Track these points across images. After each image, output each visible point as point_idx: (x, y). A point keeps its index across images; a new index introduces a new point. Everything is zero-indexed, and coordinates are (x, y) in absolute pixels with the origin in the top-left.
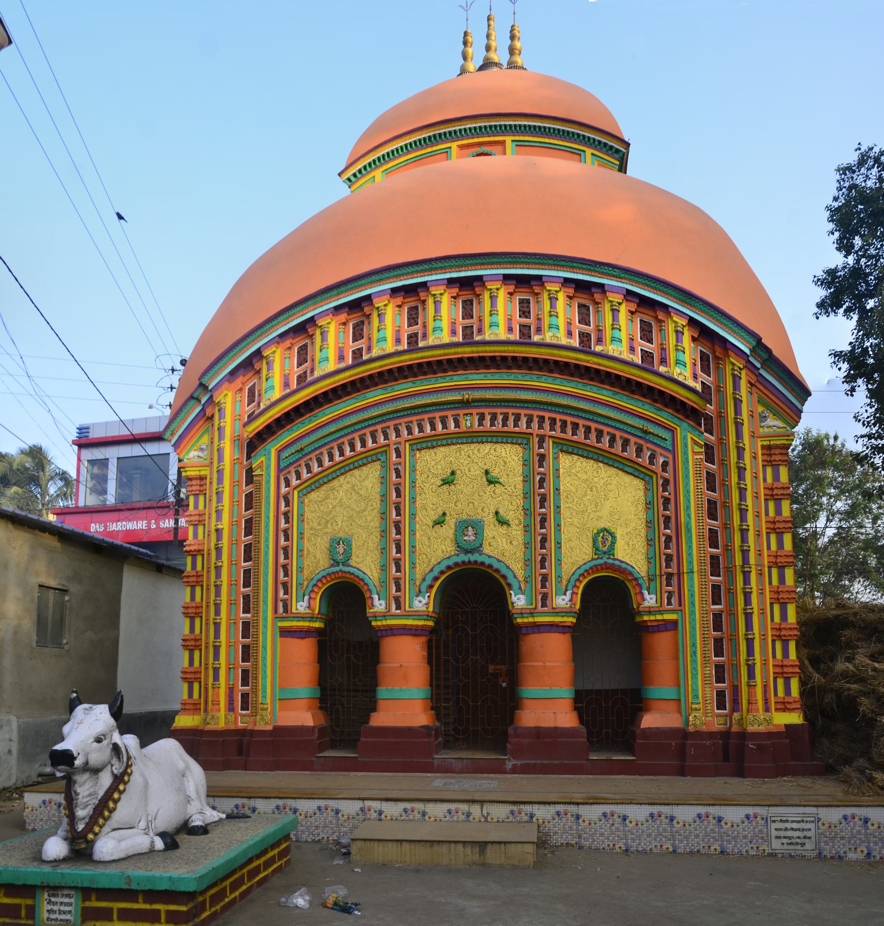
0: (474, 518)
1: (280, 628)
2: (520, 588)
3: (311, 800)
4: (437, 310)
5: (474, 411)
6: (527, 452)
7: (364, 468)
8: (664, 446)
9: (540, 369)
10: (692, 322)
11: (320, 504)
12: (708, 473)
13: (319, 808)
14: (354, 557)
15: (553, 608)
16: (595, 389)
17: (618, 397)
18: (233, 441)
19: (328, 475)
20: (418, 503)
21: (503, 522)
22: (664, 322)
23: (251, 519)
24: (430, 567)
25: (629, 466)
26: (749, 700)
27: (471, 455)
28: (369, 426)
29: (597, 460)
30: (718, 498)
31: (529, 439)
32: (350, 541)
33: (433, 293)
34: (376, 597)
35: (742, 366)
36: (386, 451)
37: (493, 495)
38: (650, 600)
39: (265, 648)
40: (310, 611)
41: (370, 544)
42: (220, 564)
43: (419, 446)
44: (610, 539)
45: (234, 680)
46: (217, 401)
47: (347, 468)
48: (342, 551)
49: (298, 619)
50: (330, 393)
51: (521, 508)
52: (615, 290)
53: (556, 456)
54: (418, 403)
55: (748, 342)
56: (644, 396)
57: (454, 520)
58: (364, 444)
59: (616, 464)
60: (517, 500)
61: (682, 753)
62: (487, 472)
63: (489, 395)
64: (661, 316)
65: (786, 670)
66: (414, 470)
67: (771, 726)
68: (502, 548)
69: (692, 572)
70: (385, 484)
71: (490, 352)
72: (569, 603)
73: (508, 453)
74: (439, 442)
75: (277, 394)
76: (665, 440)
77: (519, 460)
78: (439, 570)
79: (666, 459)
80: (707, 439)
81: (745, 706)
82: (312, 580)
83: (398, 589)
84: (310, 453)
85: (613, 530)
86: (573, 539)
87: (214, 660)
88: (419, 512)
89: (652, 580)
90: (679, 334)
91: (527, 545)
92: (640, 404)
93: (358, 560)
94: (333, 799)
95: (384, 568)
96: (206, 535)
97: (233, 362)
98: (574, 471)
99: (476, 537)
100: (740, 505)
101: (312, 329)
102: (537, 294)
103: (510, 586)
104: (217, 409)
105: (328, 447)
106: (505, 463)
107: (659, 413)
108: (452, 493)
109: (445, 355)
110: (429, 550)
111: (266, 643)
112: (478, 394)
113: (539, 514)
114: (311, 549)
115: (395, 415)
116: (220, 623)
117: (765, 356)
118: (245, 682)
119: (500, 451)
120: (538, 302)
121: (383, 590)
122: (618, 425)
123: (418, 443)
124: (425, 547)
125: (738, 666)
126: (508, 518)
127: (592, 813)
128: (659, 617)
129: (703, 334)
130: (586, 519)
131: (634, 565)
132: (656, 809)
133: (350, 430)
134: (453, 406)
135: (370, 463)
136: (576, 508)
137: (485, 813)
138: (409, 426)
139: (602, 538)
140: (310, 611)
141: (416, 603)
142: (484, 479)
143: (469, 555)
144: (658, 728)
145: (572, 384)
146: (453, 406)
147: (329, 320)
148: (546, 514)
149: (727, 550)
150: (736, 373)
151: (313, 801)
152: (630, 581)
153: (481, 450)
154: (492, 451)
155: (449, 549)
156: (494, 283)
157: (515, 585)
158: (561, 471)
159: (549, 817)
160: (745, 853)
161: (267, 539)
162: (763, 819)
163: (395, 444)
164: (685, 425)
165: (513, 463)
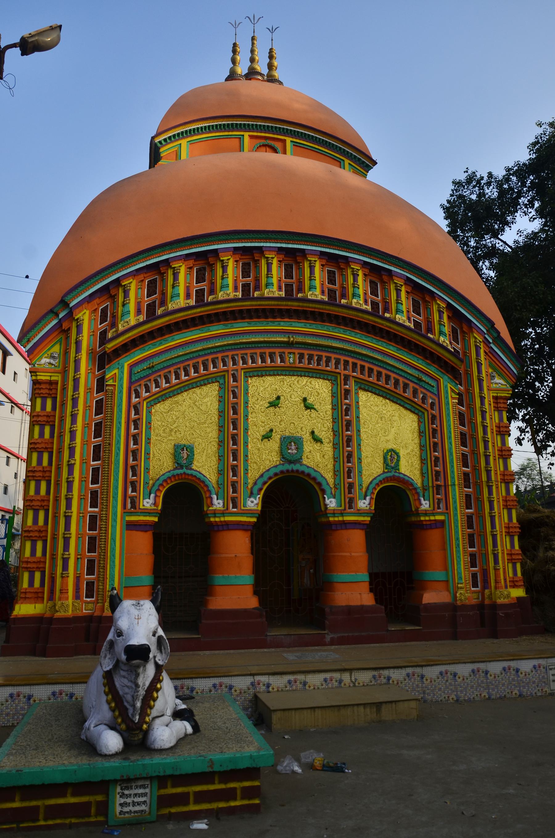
1: (128, 522)
2: (332, 493)
4: (269, 269)
5: (296, 351)
6: (335, 387)
7: (204, 387)
8: (432, 391)
9: (346, 325)
10: (449, 306)
11: (165, 415)
12: (459, 412)
13: (214, 686)
14: (195, 463)
15: (359, 510)
16: (385, 344)
17: (400, 352)
18: (88, 354)
19: (174, 390)
20: (249, 420)
21: (317, 440)
22: (430, 302)
23: (101, 423)
25: (408, 404)
27: (292, 385)
28: (211, 353)
29: (385, 398)
30: (467, 431)
31: (337, 377)
32: (193, 448)
33: (266, 256)
34: (215, 497)
35: (481, 340)
36: (224, 375)
37: (309, 418)
38: (425, 505)
39: (114, 540)
40: (155, 508)
41: (209, 451)
42: (73, 462)
44: (396, 457)
45: (81, 569)
46: (76, 318)
48: (185, 456)
49: (145, 514)
51: (331, 430)
52: (400, 276)
53: (356, 391)
54: (253, 340)
55: (486, 325)
56: (419, 353)
57: (279, 436)
58: (206, 368)
59: (399, 402)
60: (328, 423)
62: (305, 400)
63: (309, 340)
64: (427, 299)
65: (514, 557)
66: (247, 393)
67: (509, 599)
69: (454, 485)
70: (223, 402)
71: (312, 308)
72: (368, 506)
73: (320, 386)
75: (132, 320)
76: (433, 387)
78: (268, 476)
80: (459, 389)
81: (493, 584)
82: (158, 479)
83: (234, 491)
85: (398, 451)
88: (250, 428)
89: (426, 490)
90: (441, 313)
92: (416, 359)
93: (197, 464)
94: (227, 676)
95: (220, 473)
96: (56, 435)
97: (94, 286)
98: (369, 404)
99: (298, 451)
100: (483, 437)
101: (164, 268)
102: (342, 269)
103: (324, 491)
104: (74, 324)
105: (175, 367)
106: (319, 394)
107: (429, 367)
109: (278, 305)
110: (258, 460)
112: (300, 339)
113: (346, 436)
114: (157, 454)
115: (233, 347)
117: (495, 335)
118: (90, 571)
119: (314, 384)
120: (342, 275)
121: (221, 491)
122: (401, 373)
123: (251, 372)
124: (255, 457)
126: (321, 437)
127: (432, 672)
128: (432, 518)
129: (455, 315)
132: (475, 666)
133: (195, 355)
134: (279, 345)
135: (210, 383)
137: (353, 679)
138: (243, 357)
139: (391, 456)
140: (155, 508)
142: (302, 405)
143: (292, 465)
144: (435, 603)
146: (279, 345)
148: (351, 436)
149: (475, 469)
152: (410, 490)
153: (300, 382)
154: (308, 383)
155: (275, 459)
157: (328, 491)
158: (360, 403)
159: (401, 679)
160: (534, 695)
161: (118, 442)
162: (544, 668)
163: (233, 370)
164: (446, 377)
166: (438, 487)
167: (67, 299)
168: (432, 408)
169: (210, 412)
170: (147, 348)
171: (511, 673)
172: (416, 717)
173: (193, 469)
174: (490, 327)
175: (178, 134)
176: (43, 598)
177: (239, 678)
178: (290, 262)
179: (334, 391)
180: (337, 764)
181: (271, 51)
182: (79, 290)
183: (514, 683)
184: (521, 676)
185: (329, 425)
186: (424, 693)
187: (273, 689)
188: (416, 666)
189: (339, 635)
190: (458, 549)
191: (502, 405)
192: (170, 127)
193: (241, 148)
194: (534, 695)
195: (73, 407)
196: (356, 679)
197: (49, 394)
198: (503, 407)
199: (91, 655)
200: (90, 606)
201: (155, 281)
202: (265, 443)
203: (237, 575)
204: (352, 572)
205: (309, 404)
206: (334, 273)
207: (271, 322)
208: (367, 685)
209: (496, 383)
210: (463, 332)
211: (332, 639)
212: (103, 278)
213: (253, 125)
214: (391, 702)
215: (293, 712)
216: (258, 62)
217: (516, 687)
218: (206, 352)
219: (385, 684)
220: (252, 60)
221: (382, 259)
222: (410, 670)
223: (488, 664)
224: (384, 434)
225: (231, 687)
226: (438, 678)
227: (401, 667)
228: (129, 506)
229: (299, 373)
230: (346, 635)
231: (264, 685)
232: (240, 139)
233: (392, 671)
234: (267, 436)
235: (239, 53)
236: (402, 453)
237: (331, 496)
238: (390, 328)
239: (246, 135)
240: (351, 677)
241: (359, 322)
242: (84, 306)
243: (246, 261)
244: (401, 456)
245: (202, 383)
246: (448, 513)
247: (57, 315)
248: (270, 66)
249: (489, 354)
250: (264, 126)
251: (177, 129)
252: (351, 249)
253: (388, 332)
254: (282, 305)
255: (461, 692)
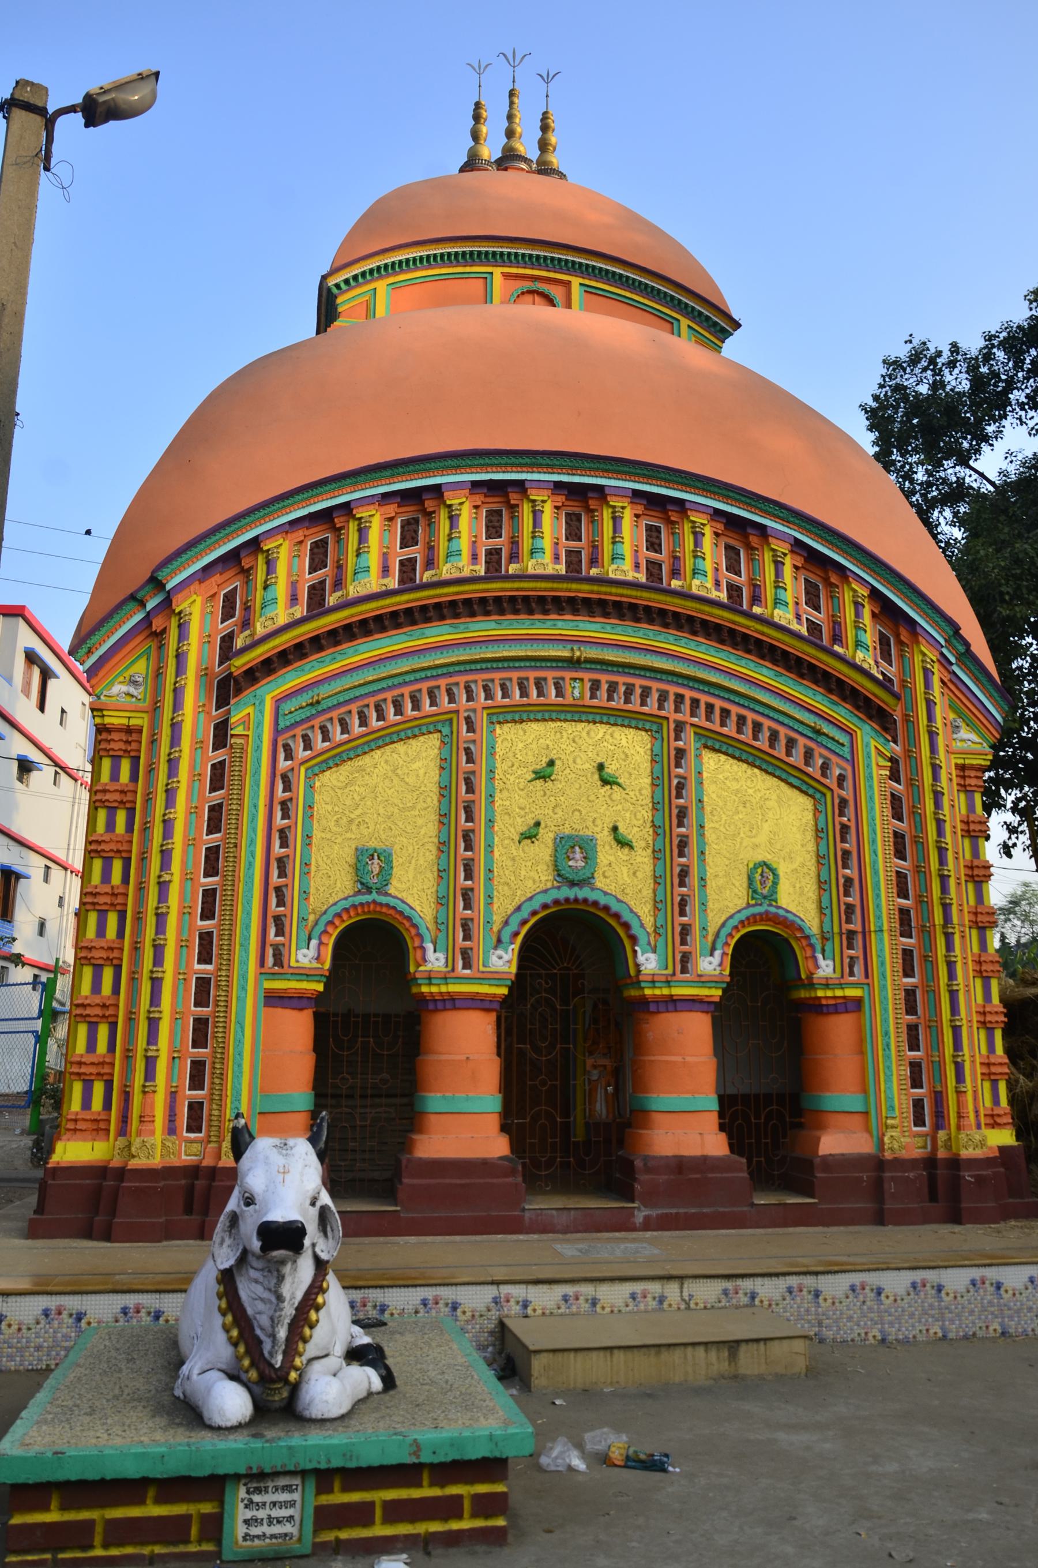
0: (581, 833)
2: (649, 943)
3: (410, 1289)
4: (537, 523)
5: (587, 676)
6: (658, 743)
7: (413, 742)
8: (841, 753)
9: (680, 628)
10: (875, 594)
11: (339, 792)
12: (892, 795)
13: (424, 1303)
14: (394, 882)
15: (700, 976)
16: (752, 665)
18: (198, 677)
19: (357, 747)
20: (497, 804)
21: (623, 843)
22: (837, 587)
23: (220, 805)
24: (515, 904)
25: (795, 777)
26: (958, 1112)
27: (577, 739)
28: (427, 678)
29: (753, 765)
30: (907, 830)
31: (661, 724)
32: (390, 855)
33: (532, 497)
34: (429, 947)
35: (934, 659)
36: (451, 720)
37: (609, 802)
38: (826, 968)
39: (241, 1025)
40: (319, 966)
41: (421, 862)
42: (166, 878)
43: (501, 718)
44: (771, 877)
45: (179, 1078)
47: (388, 740)
48: (376, 870)
49: (298, 977)
50: (371, 622)
51: (649, 824)
52: (781, 537)
53: (698, 752)
54: (506, 654)
55: (944, 631)
56: (816, 682)
57: (552, 835)
59: (778, 773)
60: (644, 812)
61: (878, 1189)
62: (601, 767)
63: (610, 655)
64: (834, 579)
65: (993, 1069)
67: (985, 1149)
68: (621, 882)
69: (882, 931)
70: (448, 769)
71: (616, 595)
72: (718, 968)
74: (532, 717)
76: (843, 745)
77: (645, 753)
78: (529, 910)
79: (843, 772)
80: (893, 751)
82: (325, 913)
83: (467, 937)
84: (330, 709)
85: (774, 866)
86: (721, 874)
87: (149, 1043)
88: (498, 818)
89: (827, 939)
90: (858, 606)
91: (657, 880)
92: (810, 693)
93: (398, 885)
94: (448, 1285)
95: (441, 902)
96: (136, 827)
97: (212, 551)
98: (720, 776)
99: (586, 863)
101: (342, 519)
103: (634, 939)
104: (174, 622)
106: (627, 756)
107: (835, 708)
108: (548, 793)
109: (552, 590)
110: (513, 878)
111: (244, 1017)
113: (678, 836)
114: (323, 866)
115: (468, 667)
116: (160, 980)
117: (962, 649)
118: (197, 1082)
119: (618, 738)
121: (442, 936)
122: (781, 718)
124: (507, 872)
125: (942, 1064)
126: (630, 837)
127: (835, 1286)
128: (839, 993)
129: (887, 611)
130: (738, 846)
131: (802, 916)
132: (918, 1276)
133: (396, 681)
134: (554, 665)
135: (424, 734)
136: (724, 830)
137: (686, 1295)
139: (762, 875)
140: (319, 966)
141: (494, 959)
142: (596, 776)
143: (576, 889)
144: (843, 1155)
145: (722, 655)
147: (374, 512)
148: (687, 836)
149: (921, 902)
150: (929, 666)
151: (414, 1289)
152: (798, 939)
153: (592, 734)
155: (543, 878)
156: (620, 499)
157: (642, 938)
158: (705, 775)
159: (777, 1297)
160: (1031, 1333)
161: (252, 842)
163: (467, 710)
164: (867, 728)
165: (637, 757)
166: (851, 934)
167: (161, 576)
168: (840, 786)
169: (423, 788)
170: (308, 667)
171: (985, 1291)
172: (804, 1371)
173: (390, 895)
174: (952, 633)
175: (371, 271)
176: (108, 1130)
177: (470, 1288)
178: (577, 510)
179: (657, 750)
180: (653, 1455)
181: (545, 116)
182: (183, 559)
183: (992, 1309)
184: (1005, 1296)
185: (646, 815)
186: (820, 1324)
187: (534, 1310)
188: (805, 1273)
189: (660, 1211)
190: (887, 1052)
191: (973, 782)
192: (356, 257)
193: (487, 298)
194: (1031, 1333)
195: (169, 777)
196: (691, 1296)
197: (125, 751)
198: (976, 786)
199: (195, 1239)
200: (196, 1147)
201: (324, 542)
202: (526, 848)
203: (470, 1095)
204: (687, 1092)
205: (609, 775)
206: (658, 530)
207: (539, 620)
208: (713, 1307)
209: (962, 740)
210: (900, 643)
211: (647, 1218)
212: (229, 537)
213: (509, 254)
214: (757, 1341)
215: (572, 1355)
216: (520, 137)
217: (997, 1317)
218: (418, 676)
219: (746, 1306)
220: (510, 134)
221: (749, 504)
222: (793, 1281)
223: (943, 1271)
224: (749, 834)
225: (455, 1307)
226: (847, 1297)
227: (777, 1275)
228: (270, 960)
229: (591, 717)
230: (674, 1211)
231: (518, 1303)
232: (486, 279)
233: (759, 1281)
234: (530, 835)
235: (485, 120)
236: (782, 869)
237: (648, 948)
238: (763, 634)
239: (498, 272)
240: (681, 1292)
241: (704, 623)
242: (192, 588)
243: (495, 507)
244: (781, 872)
245: (409, 733)
246: (868, 984)
247: (142, 604)
248: (544, 145)
249: (950, 685)
250: (531, 256)
251: (369, 261)
252: (691, 486)
253: (759, 642)
254: (561, 590)
255: (891, 1324)
